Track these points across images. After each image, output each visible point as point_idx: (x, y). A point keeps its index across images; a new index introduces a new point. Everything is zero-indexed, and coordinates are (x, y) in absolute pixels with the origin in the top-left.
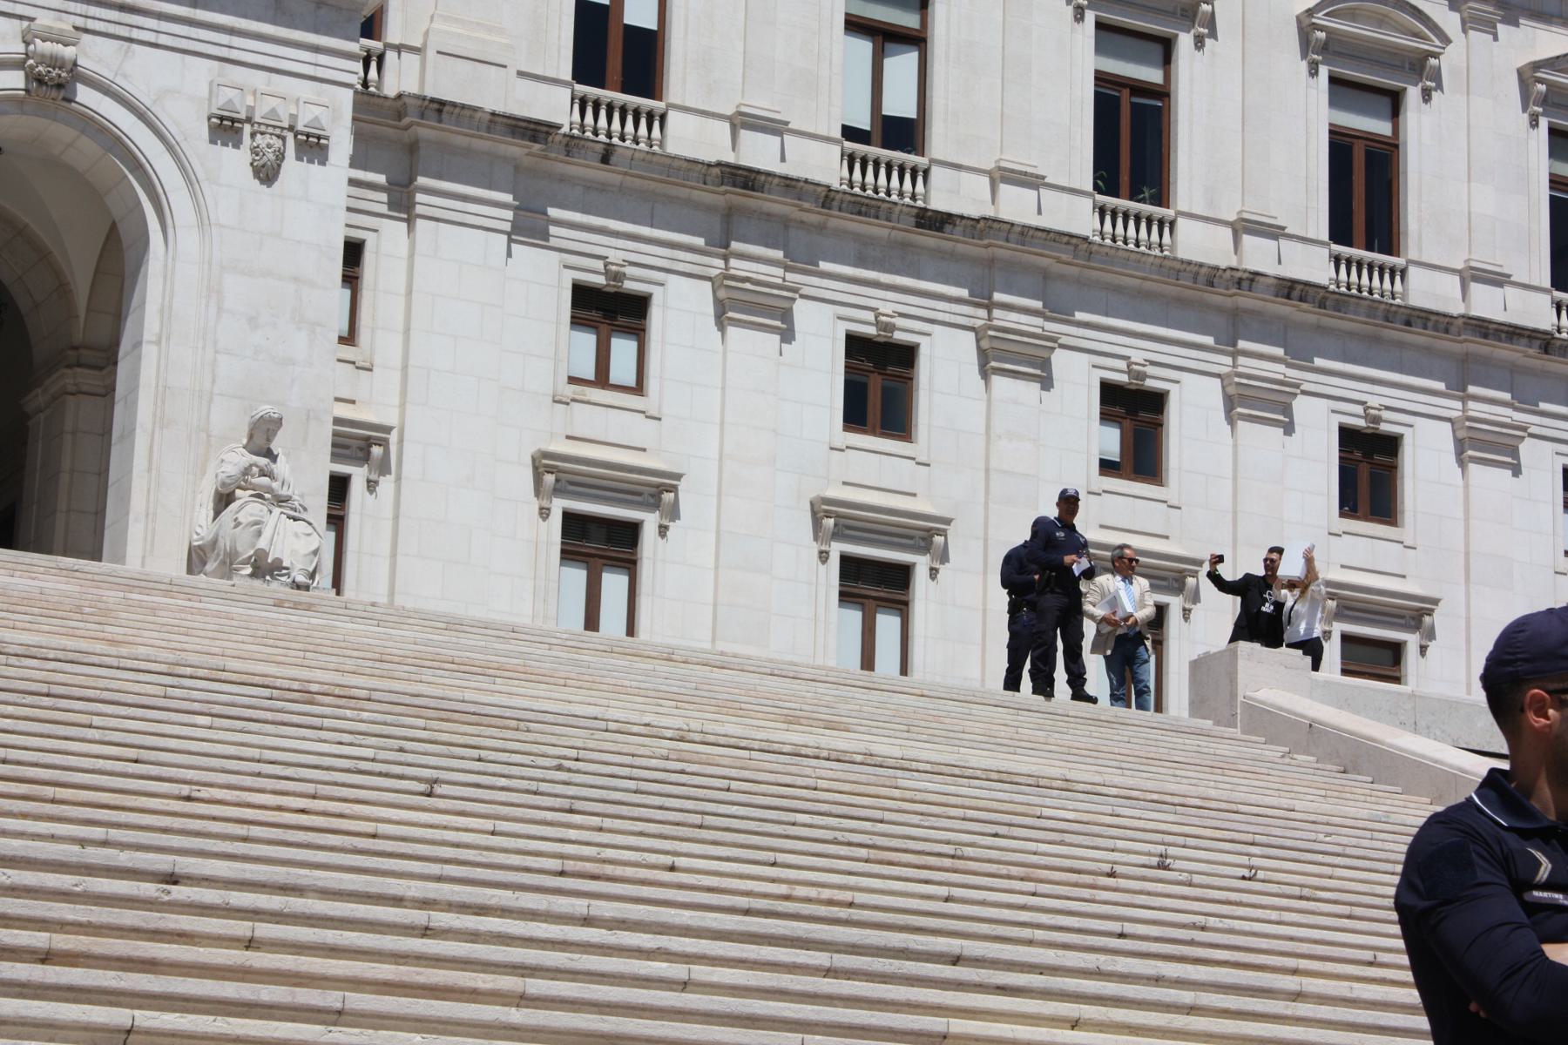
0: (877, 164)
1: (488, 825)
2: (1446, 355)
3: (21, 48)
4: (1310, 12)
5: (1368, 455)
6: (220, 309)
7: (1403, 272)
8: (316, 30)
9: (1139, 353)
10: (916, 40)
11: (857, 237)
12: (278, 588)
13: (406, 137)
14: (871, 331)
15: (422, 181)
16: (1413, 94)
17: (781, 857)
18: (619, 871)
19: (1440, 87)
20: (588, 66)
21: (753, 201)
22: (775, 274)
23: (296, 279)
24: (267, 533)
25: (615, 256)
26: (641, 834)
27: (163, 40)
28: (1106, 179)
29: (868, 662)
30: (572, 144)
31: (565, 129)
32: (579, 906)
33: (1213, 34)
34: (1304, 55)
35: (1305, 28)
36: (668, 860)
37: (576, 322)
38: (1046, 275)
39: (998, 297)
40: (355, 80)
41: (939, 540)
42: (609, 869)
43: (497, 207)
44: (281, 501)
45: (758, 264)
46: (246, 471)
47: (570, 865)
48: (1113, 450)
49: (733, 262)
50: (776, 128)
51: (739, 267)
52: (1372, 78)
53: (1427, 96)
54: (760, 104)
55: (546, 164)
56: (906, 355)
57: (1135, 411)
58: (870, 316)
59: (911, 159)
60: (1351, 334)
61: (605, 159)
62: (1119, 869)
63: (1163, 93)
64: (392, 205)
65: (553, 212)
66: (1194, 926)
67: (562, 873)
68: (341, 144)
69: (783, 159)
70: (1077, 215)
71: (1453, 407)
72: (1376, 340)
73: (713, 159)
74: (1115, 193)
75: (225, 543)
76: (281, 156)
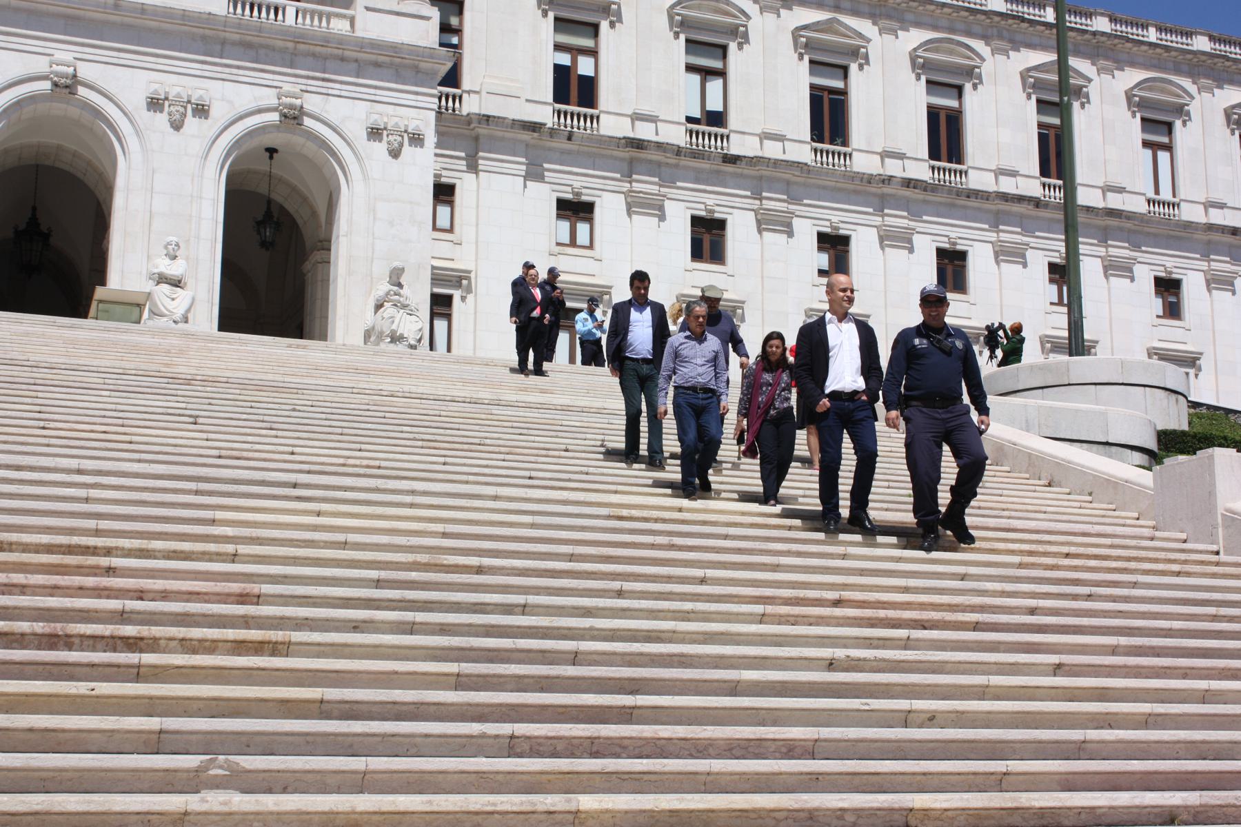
0: (703, 134)
1: (204, 436)
2: (988, 211)
3: (276, 101)
4: (915, 50)
5: (951, 261)
6: (374, 218)
7: (966, 173)
8: (416, 85)
9: (836, 217)
10: (721, 74)
11: (694, 169)
12: (401, 347)
13: (473, 133)
14: (703, 213)
15: (481, 154)
16: (968, 87)
17: (363, 447)
19: (981, 82)
20: (561, 94)
21: (643, 155)
22: (654, 189)
23: (411, 203)
24: (396, 321)
25: (577, 185)
26: (298, 438)
27: (343, 93)
28: (817, 133)
31: (550, 125)
32: (73, 463)
33: (868, 63)
34: (913, 71)
35: (913, 58)
36: (290, 449)
37: (559, 216)
38: (788, 183)
39: (764, 194)
40: (436, 107)
41: (739, 311)
42: (245, 454)
43: (518, 165)
44: (404, 306)
45: (646, 185)
46: (388, 294)
48: (825, 266)
49: (634, 184)
50: (653, 119)
51: (637, 186)
52: (947, 81)
53: (975, 87)
54: (645, 109)
55: (541, 143)
56: (721, 224)
58: (702, 207)
59: (720, 130)
60: (941, 203)
61: (569, 139)
62: (570, 447)
63: (844, 92)
64: (468, 166)
65: (546, 166)
66: (582, 473)
67: (220, 457)
68: (431, 138)
69: (657, 134)
71: (993, 236)
75: (378, 328)
76: (401, 145)
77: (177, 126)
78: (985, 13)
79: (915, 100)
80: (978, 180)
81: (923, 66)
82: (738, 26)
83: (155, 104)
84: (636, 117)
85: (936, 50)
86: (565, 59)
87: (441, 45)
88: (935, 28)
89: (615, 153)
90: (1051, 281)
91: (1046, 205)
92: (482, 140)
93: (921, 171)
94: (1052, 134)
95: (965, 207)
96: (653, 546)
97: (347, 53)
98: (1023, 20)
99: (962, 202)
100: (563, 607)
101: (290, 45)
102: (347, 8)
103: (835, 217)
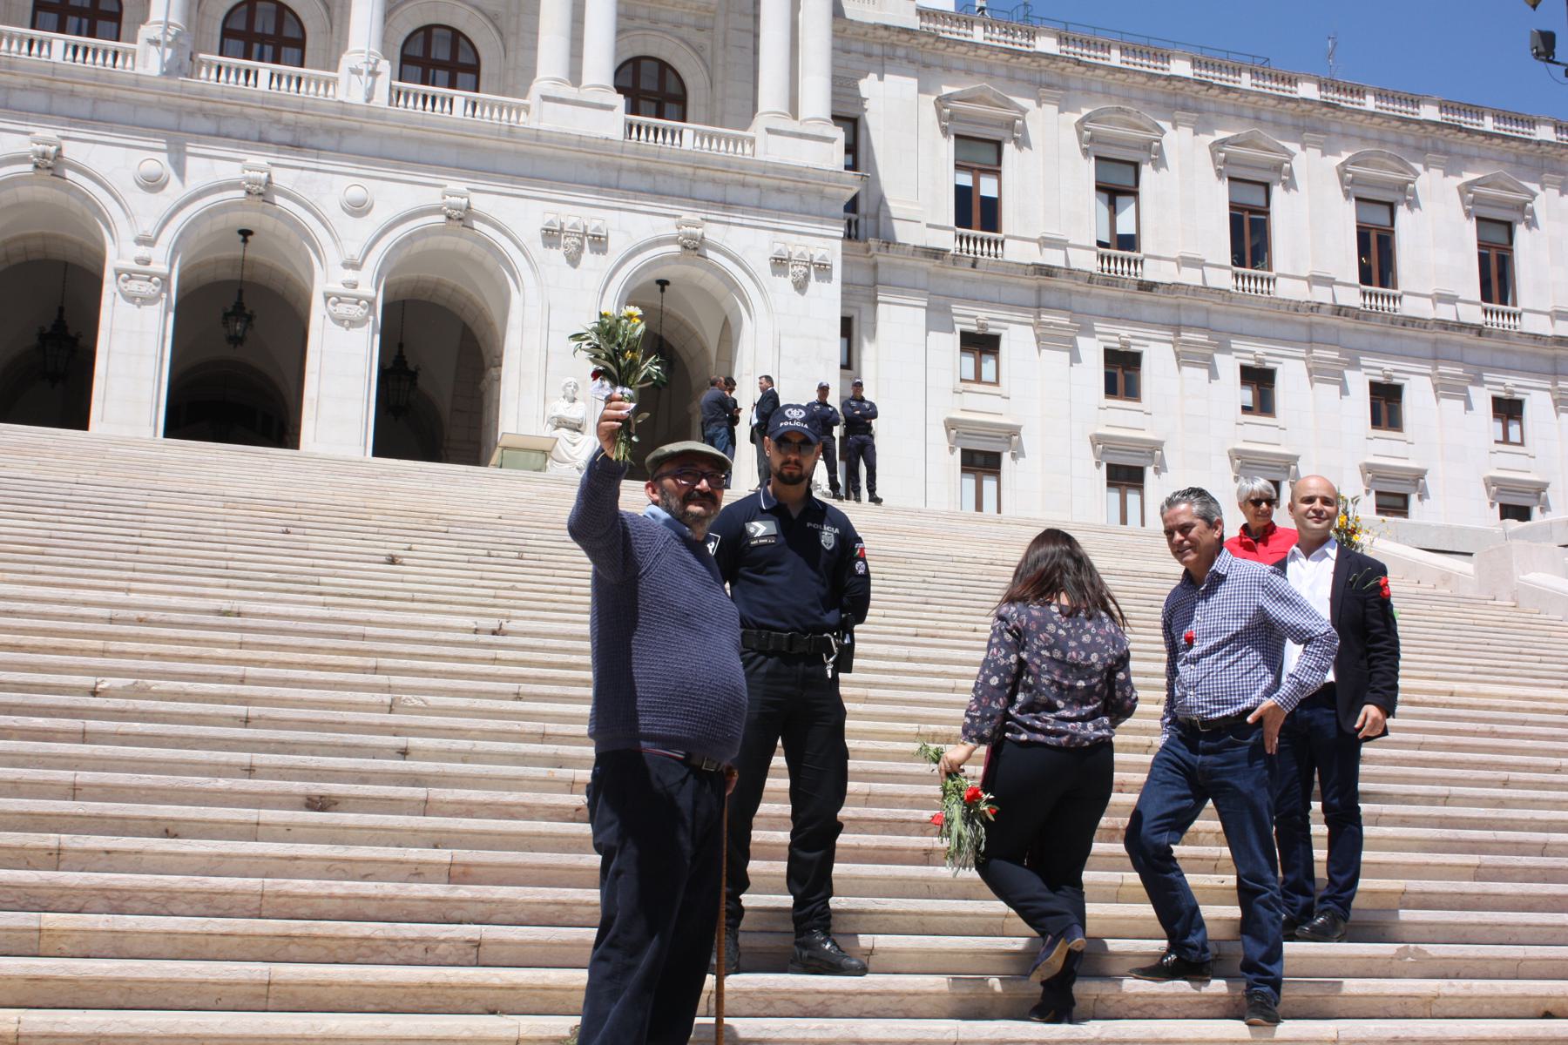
4: (1343, 164)
10: (1133, 193)
11: (1107, 297)
18: (946, 633)
20: (963, 219)
21: (1052, 282)
28: (1238, 258)
29: (1124, 521)
30: (956, 259)
42: (941, 632)
47: (920, 631)
48: (1249, 402)
54: (1054, 232)
57: (1259, 380)
70: (1223, 279)
72: (1387, 334)
73: (1029, 262)
74: (1243, 266)
76: (807, 276)
77: (574, 261)
78: (1418, 122)
79: (1344, 220)
80: (1410, 307)
81: (1352, 182)
82: (1151, 142)
83: (551, 236)
84: (1046, 243)
85: (1366, 164)
86: (966, 180)
87: (847, 168)
88: (1364, 139)
89: (1022, 281)
90: (1495, 416)
91: (1490, 333)
92: (880, 270)
93: (1473, 314)
94: (1493, 254)
95: (1401, 336)
96: (1475, 733)
97: (749, 179)
98: (1460, 129)
99: (1397, 330)
100: (1480, 798)
101: (689, 171)
102: (746, 126)
103: (1509, 384)
